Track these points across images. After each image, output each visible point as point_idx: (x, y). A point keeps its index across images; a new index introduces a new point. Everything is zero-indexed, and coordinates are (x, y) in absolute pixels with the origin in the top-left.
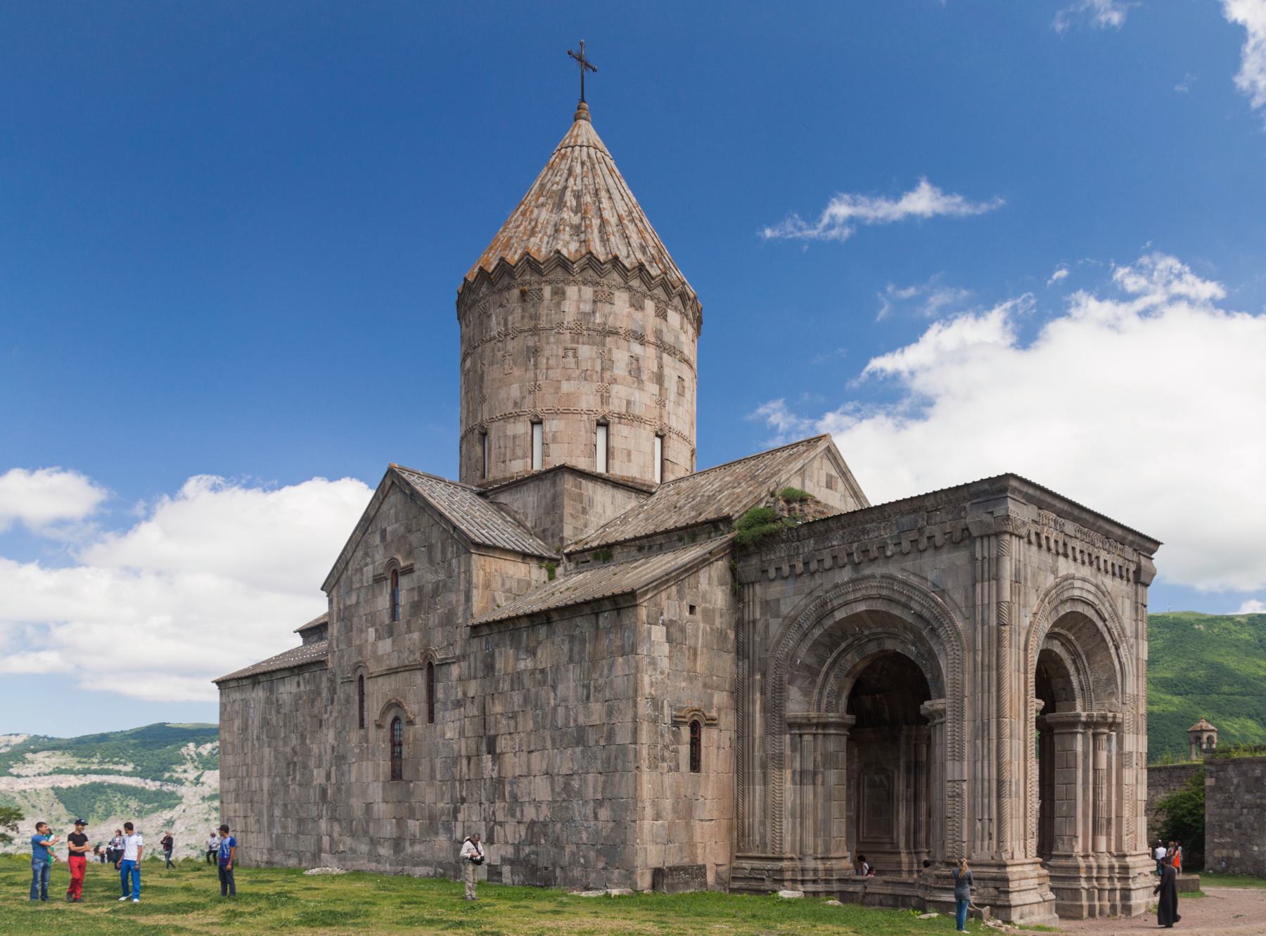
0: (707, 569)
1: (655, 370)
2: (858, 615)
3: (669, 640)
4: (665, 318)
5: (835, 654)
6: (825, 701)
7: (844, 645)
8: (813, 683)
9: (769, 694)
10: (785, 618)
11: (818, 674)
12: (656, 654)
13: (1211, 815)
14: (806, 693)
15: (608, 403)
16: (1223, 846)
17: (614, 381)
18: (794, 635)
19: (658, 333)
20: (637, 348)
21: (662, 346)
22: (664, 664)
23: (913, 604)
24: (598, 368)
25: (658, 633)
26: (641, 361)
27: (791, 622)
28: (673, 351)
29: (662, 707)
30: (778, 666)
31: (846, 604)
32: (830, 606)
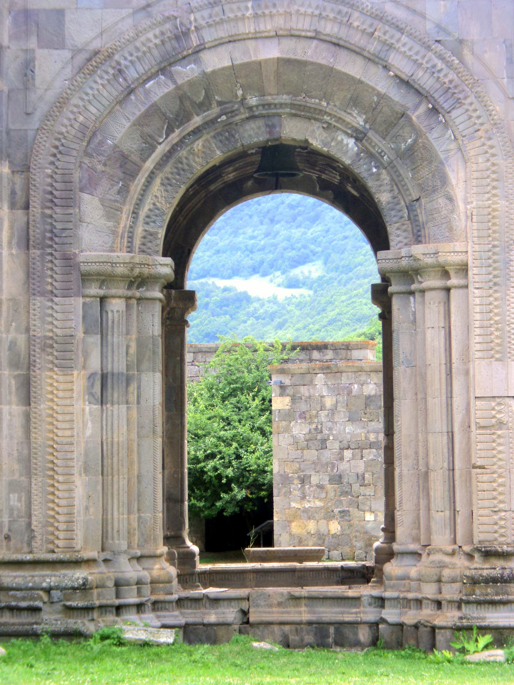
2: (257, 67)
5: (175, 137)
6: (139, 231)
7: (197, 120)
8: (124, 191)
9: (36, 209)
10: (76, 51)
11: (132, 175)
13: (283, 462)
14: (112, 212)
16: (309, 514)
18: (102, 89)
23: (395, 60)
27: (93, 61)
30: (59, 151)
31: (232, 40)
32: (194, 41)
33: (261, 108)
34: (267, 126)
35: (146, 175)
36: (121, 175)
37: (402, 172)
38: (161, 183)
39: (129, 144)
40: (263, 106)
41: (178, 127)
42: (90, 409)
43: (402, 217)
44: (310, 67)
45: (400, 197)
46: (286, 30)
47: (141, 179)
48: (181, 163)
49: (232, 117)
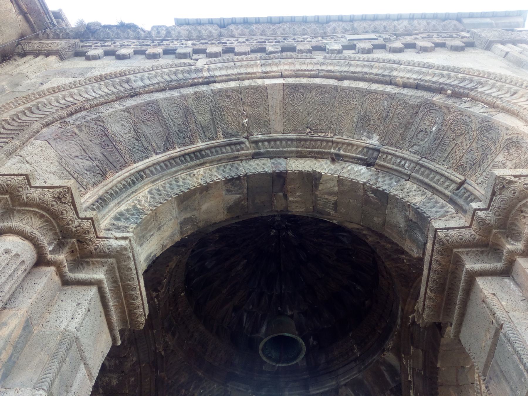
7: (201, 145)
33: (266, 143)
34: (273, 163)
35: (132, 172)
36: (99, 156)
37: (431, 167)
38: (149, 192)
39: (117, 129)
40: (269, 141)
41: (179, 147)
43: (447, 212)
44: (315, 92)
45: (436, 197)
46: (291, 71)
47: (124, 173)
48: (177, 182)
49: (238, 150)
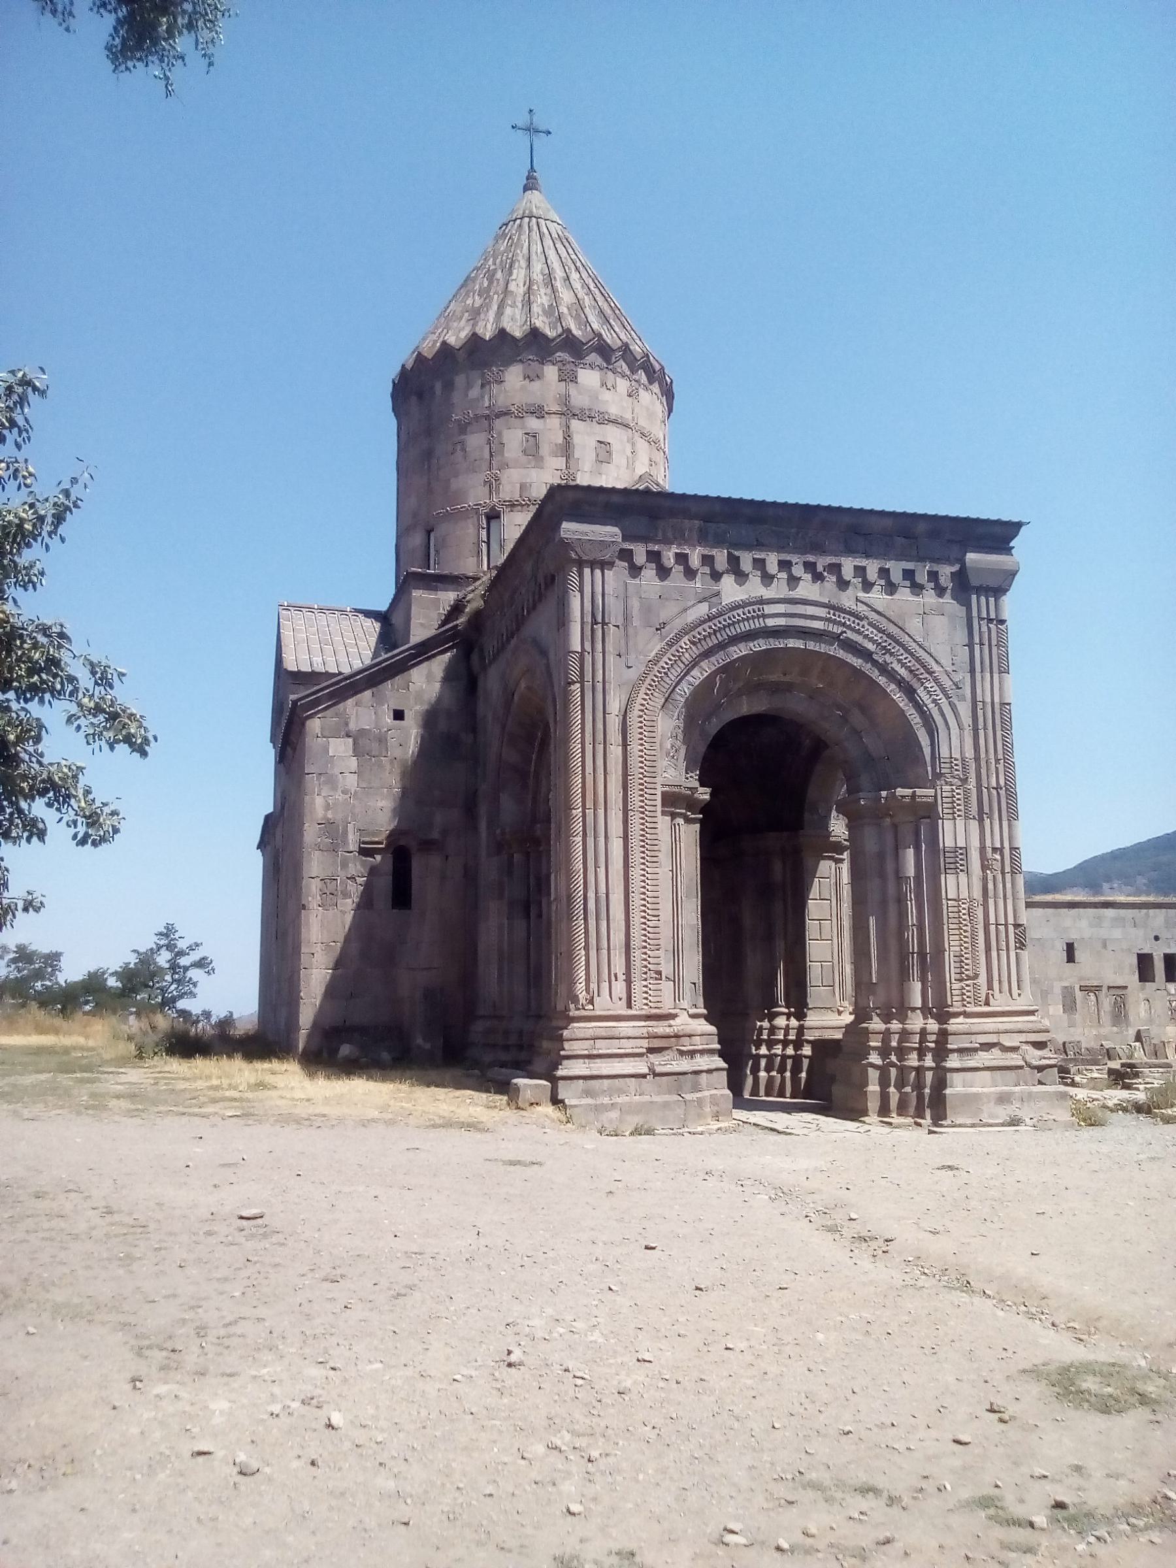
0: (425, 664)
1: (560, 440)
3: (357, 752)
4: (574, 379)
12: (336, 771)
15: (498, 492)
17: (505, 465)
19: (565, 400)
20: (533, 423)
21: (569, 412)
22: (351, 781)
24: (487, 456)
25: (340, 748)
26: (541, 438)
28: (585, 415)
29: (345, 832)
42: (506, 922)
